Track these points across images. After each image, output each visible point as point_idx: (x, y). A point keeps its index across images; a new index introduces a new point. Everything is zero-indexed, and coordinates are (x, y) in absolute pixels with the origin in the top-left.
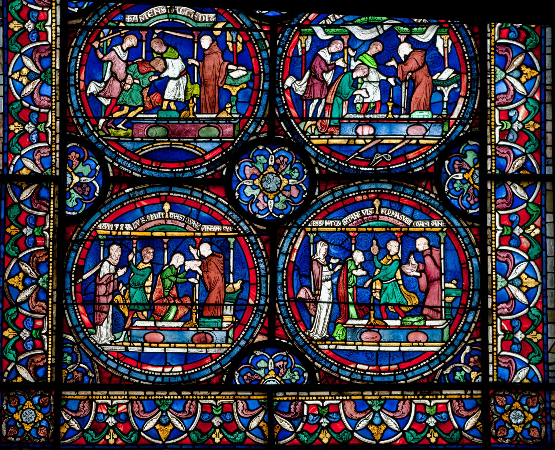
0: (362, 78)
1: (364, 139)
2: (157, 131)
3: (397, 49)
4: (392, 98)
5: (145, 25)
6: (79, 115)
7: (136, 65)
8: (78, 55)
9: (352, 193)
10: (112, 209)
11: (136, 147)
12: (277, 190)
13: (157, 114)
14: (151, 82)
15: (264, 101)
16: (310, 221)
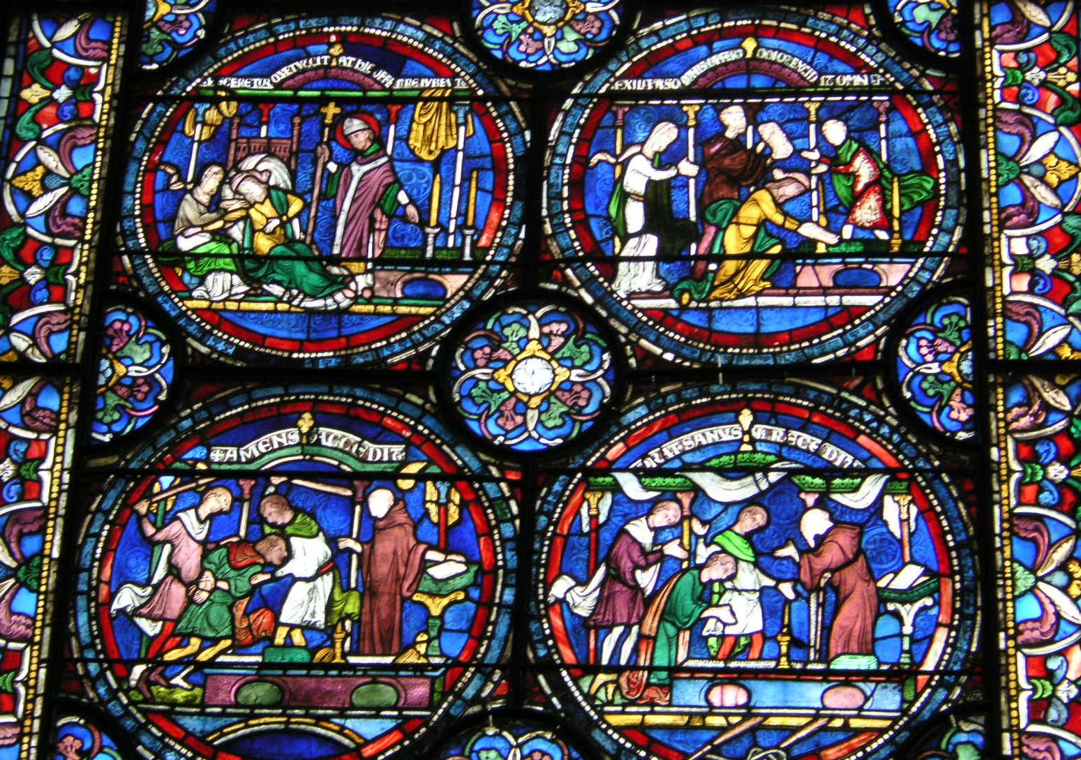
0: (721, 582)
3: (798, 522)
4: (789, 626)
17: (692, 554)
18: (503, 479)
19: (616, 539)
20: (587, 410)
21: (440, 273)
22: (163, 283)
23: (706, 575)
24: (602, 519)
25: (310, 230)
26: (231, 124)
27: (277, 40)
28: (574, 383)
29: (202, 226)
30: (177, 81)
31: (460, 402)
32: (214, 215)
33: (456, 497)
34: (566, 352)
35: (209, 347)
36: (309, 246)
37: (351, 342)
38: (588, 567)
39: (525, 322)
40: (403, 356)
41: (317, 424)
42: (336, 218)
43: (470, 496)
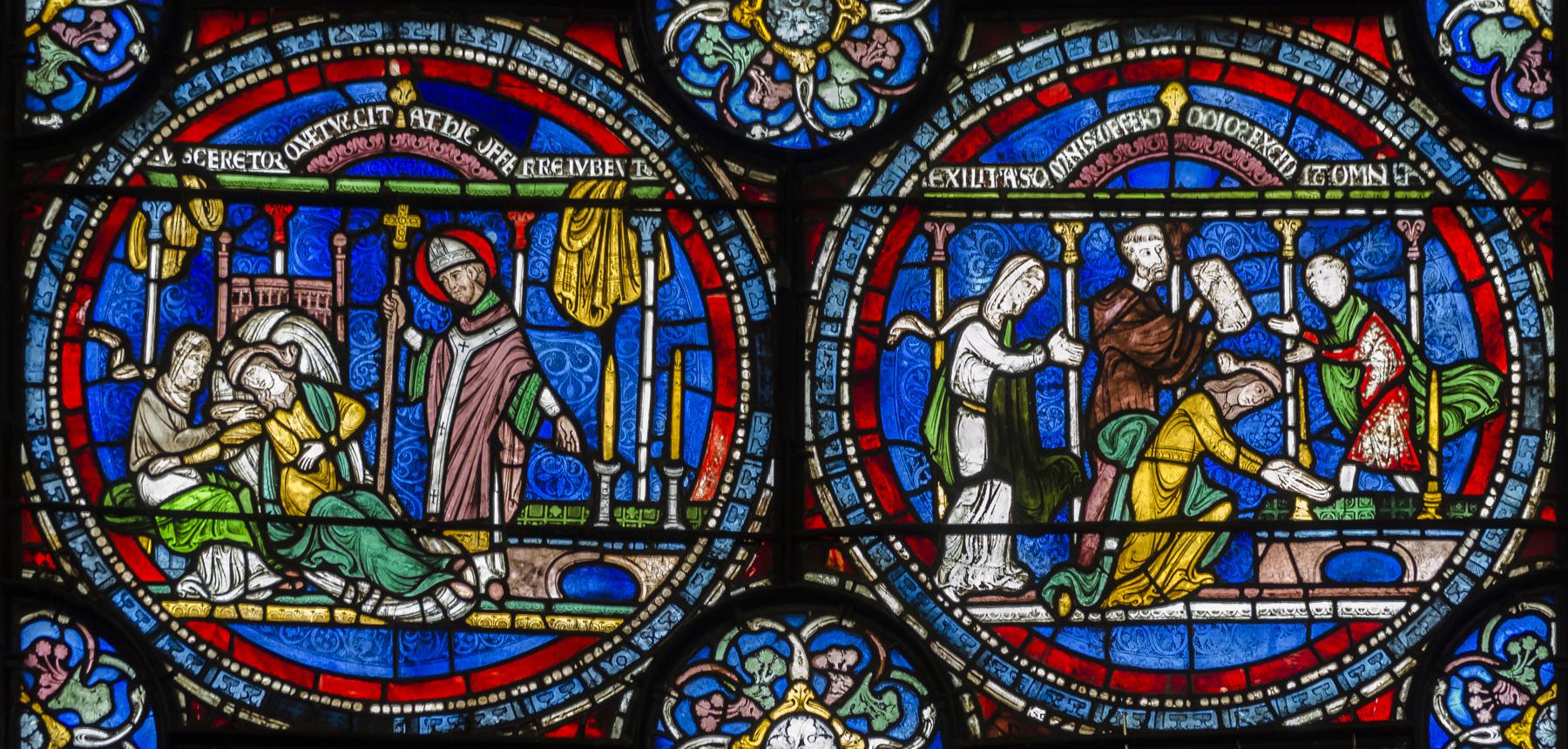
21: (625, 553)
22: (120, 568)
25: (382, 465)
26: (217, 246)
27: (288, 70)
29: (181, 455)
30: (104, 153)
32: (202, 434)
34: (857, 705)
35: (218, 691)
39: (783, 646)
40: (569, 712)
42: (429, 442)
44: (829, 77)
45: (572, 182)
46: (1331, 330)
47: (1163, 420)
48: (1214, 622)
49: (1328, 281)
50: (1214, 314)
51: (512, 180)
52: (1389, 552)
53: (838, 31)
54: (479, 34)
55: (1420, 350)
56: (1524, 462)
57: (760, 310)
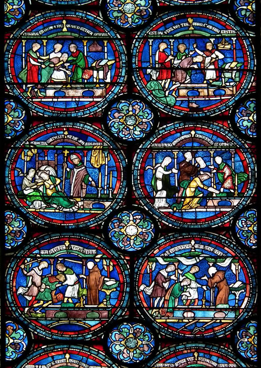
0: (186, 286)
1: (188, 320)
2: (61, 314)
4: (205, 297)
5: (53, 256)
6: (13, 305)
7: (47, 278)
8: (12, 272)
9: (181, 349)
10: (34, 357)
11: (48, 323)
12: (135, 347)
13: (61, 305)
14: (57, 288)
15: (127, 298)
16: (155, 364)
17: (178, 278)
18: (125, 259)
19: (157, 275)
20: (147, 240)
21: (103, 201)
23: (182, 284)
24: (153, 269)
26: (36, 156)
28: (144, 232)
29: (30, 187)
30: (18, 142)
31: (111, 238)
32: (34, 184)
33: (112, 264)
34: (141, 224)
35: (37, 222)
36: (63, 193)
37: (78, 221)
38: (150, 282)
39: (129, 215)
40: (94, 225)
41: (70, 244)
42: (71, 185)
43: (115, 264)
44: (136, 130)
45: (94, 146)
46: (219, 167)
47: (191, 181)
48: (200, 212)
49: (219, 160)
50: (200, 165)
51: (84, 146)
52: (229, 201)
53: (137, 123)
54: (78, 124)
55: (234, 170)
56: (252, 187)
57: (124, 165)
